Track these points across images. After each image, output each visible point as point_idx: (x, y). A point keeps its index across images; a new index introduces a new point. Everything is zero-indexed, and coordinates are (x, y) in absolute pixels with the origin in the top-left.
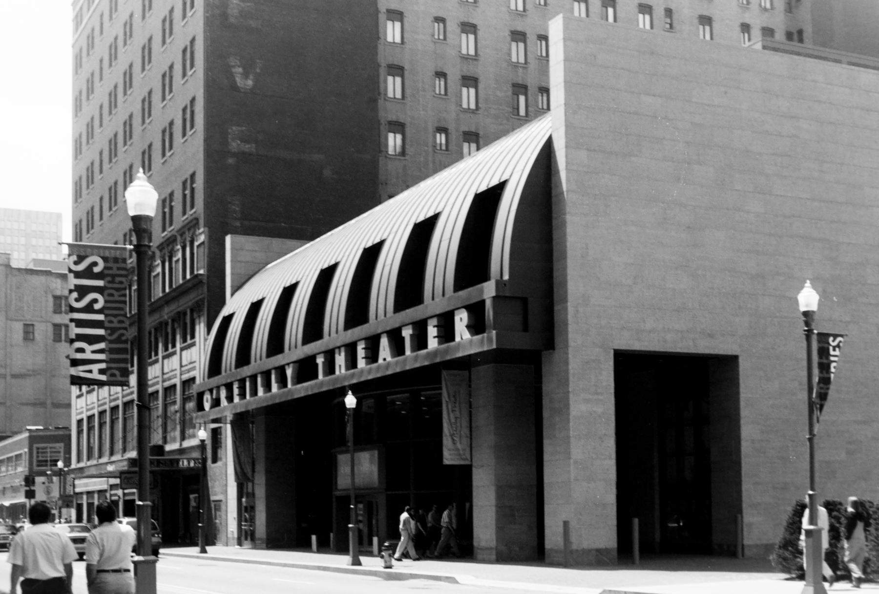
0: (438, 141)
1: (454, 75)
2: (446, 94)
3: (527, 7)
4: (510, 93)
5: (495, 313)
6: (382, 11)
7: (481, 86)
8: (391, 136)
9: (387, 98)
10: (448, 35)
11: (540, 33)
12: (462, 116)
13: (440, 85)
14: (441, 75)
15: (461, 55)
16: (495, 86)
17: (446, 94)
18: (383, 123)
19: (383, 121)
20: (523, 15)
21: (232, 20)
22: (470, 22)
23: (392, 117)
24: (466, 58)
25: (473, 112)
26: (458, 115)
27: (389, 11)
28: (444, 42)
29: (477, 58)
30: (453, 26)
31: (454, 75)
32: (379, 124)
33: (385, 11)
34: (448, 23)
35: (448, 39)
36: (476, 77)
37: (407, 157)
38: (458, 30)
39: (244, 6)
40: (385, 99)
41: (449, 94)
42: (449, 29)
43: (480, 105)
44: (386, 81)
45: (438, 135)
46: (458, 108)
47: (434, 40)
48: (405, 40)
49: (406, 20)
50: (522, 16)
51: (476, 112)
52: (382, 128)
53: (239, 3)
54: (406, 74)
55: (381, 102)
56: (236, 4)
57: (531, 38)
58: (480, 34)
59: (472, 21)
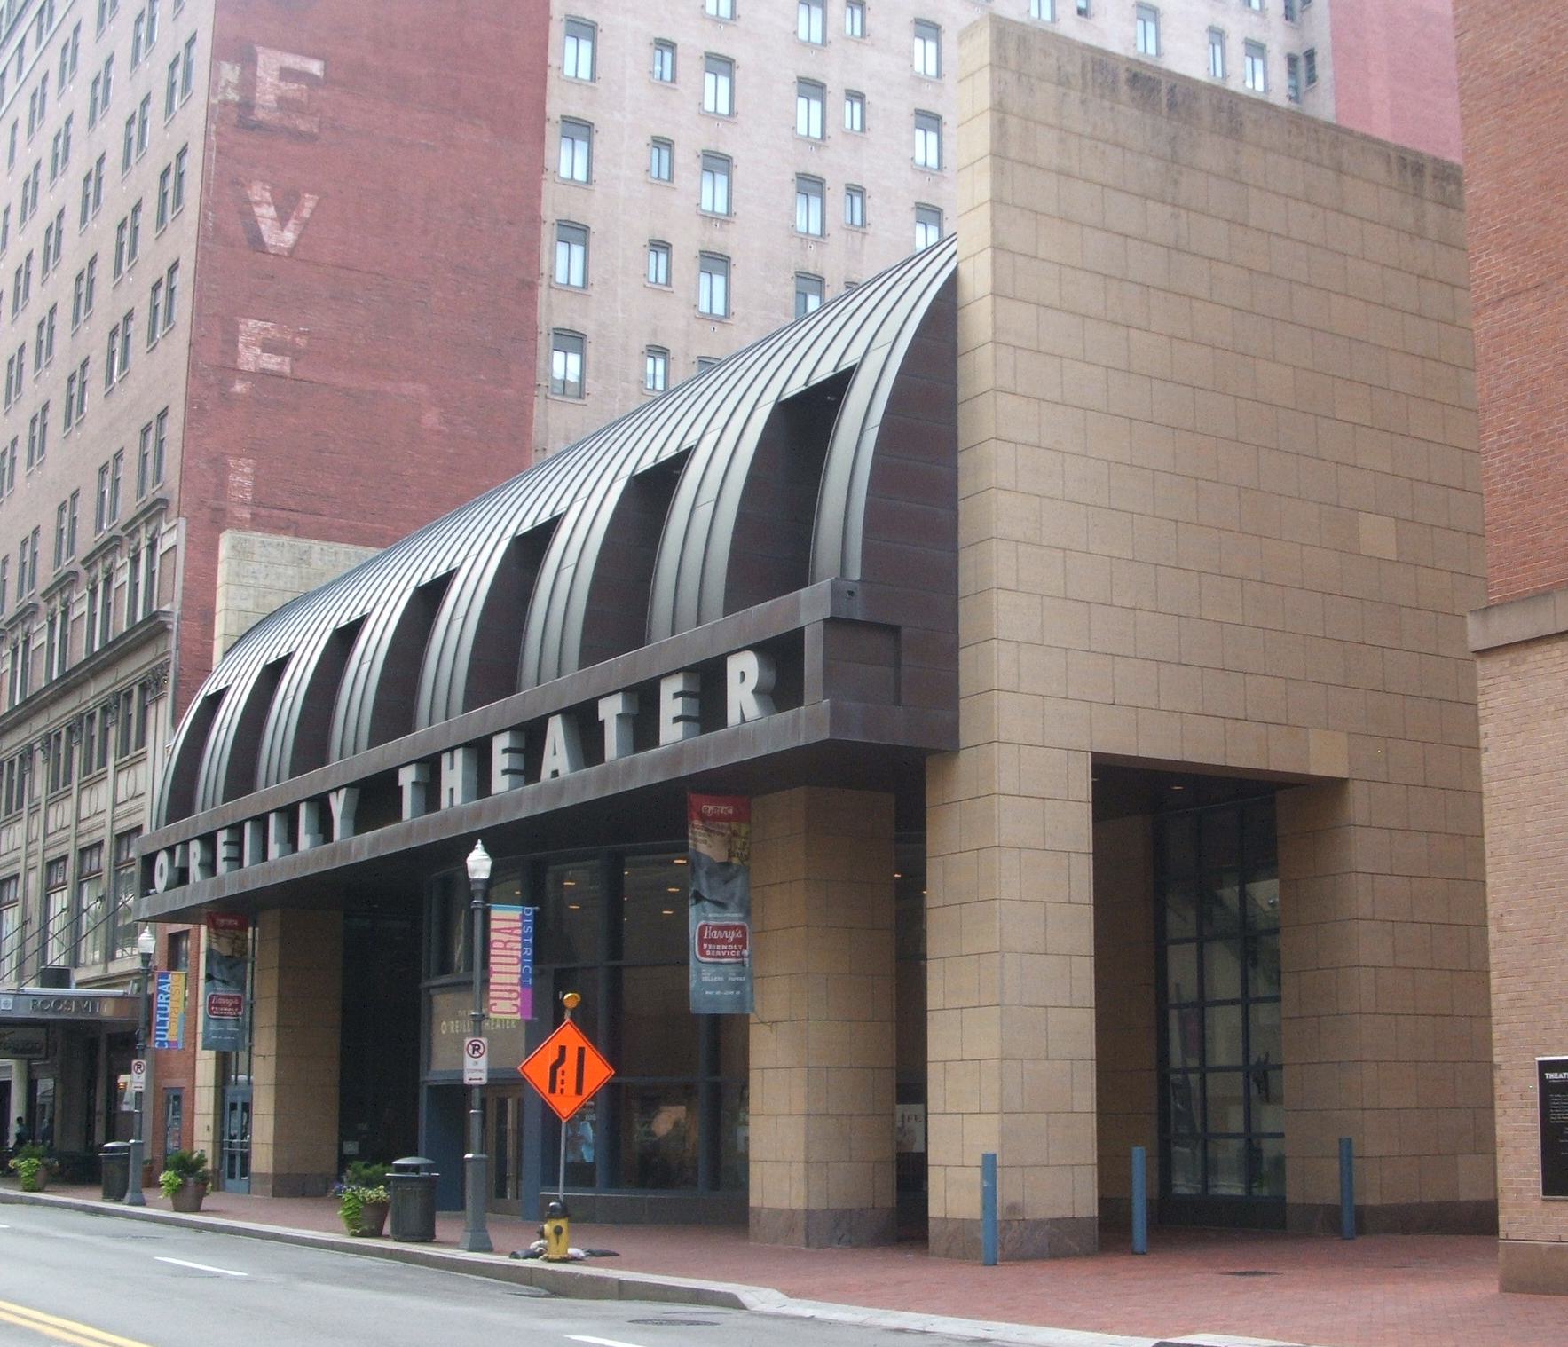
0: (650, 370)
1: (686, 245)
2: (668, 283)
3: (829, 132)
4: (791, 289)
5: (120, 1140)
6: (552, 119)
7: (736, 274)
8: (558, 357)
9: (553, 284)
10: (676, 171)
11: (850, 181)
12: (697, 326)
13: (656, 265)
14: (660, 246)
15: (700, 212)
16: (762, 274)
17: (668, 283)
18: (545, 332)
19: (543, 328)
20: (820, 146)
21: (260, 115)
22: (720, 151)
23: (561, 322)
24: (710, 218)
25: (720, 320)
26: (689, 324)
27: (565, 120)
28: (668, 184)
29: (728, 219)
30: (686, 158)
31: (686, 245)
32: (535, 332)
33: (559, 119)
34: (678, 150)
35: (675, 180)
36: (727, 254)
37: (587, 400)
38: (698, 165)
39: (285, 88)
40: (551, 287)
41: (673, 283)
42: (679, 159)
43: (733, 309)
44: (553, 252)
45: (650, 361)
46: (692, 311)
47: (650, 180)
48: (594, 176)
49: (597, 138)
50: (818, 147)
51: (725, 321)
52: (541, 340)
53: (276, 82)
54: (593, 240)
55: (542, 292)
56: (272, 84)
57: (835, 193)
58: (737, 174)
59: (725, 149)
